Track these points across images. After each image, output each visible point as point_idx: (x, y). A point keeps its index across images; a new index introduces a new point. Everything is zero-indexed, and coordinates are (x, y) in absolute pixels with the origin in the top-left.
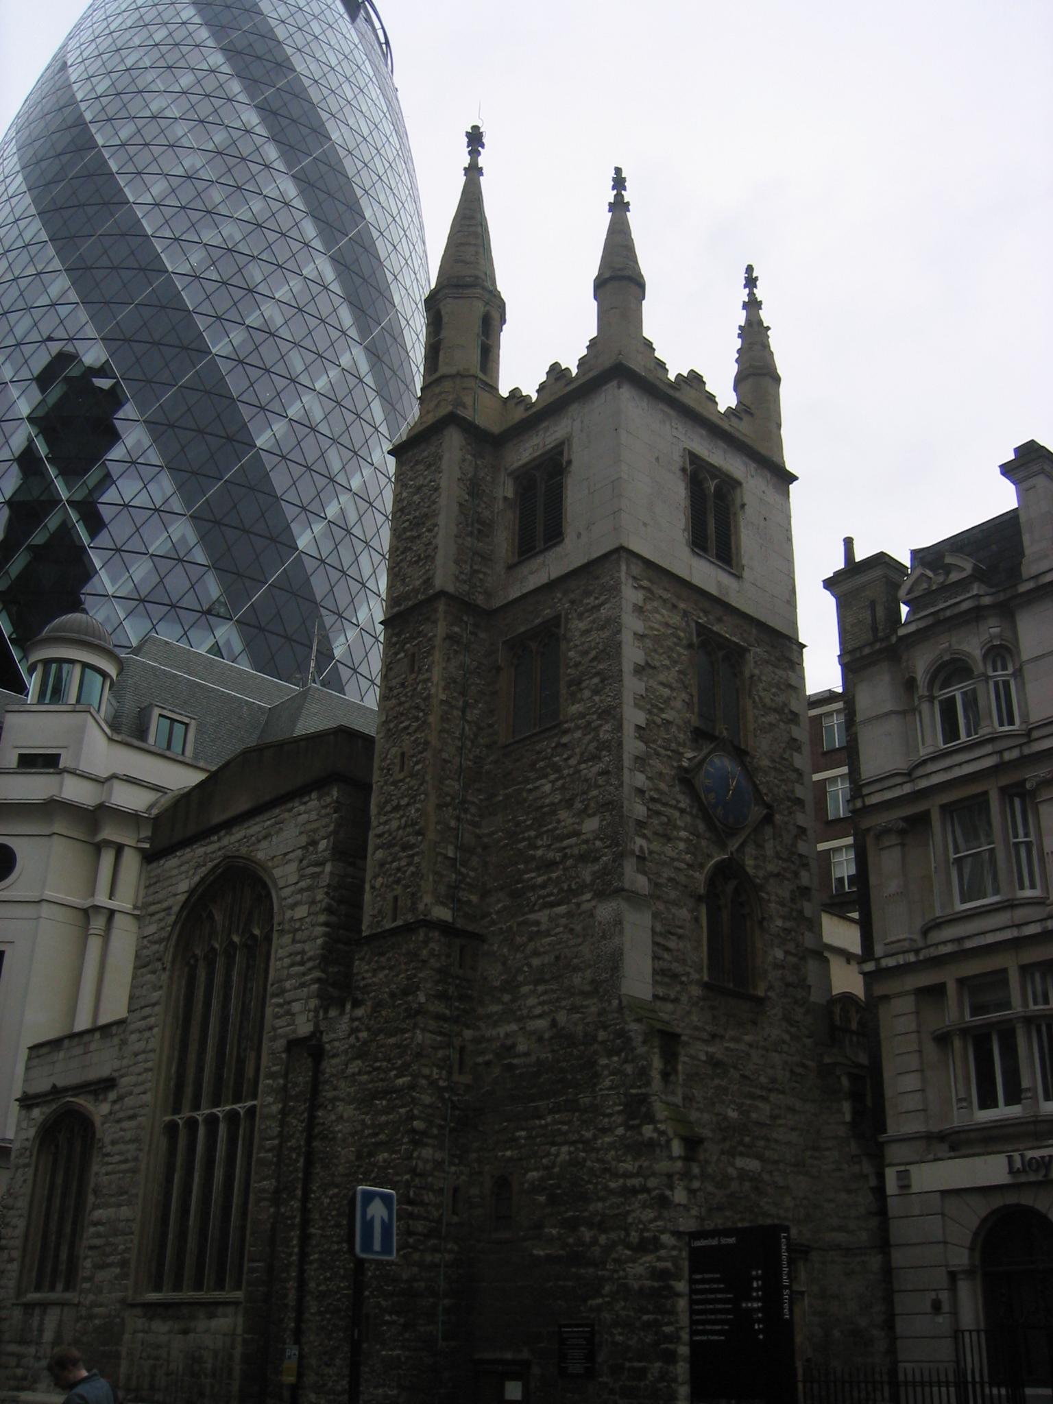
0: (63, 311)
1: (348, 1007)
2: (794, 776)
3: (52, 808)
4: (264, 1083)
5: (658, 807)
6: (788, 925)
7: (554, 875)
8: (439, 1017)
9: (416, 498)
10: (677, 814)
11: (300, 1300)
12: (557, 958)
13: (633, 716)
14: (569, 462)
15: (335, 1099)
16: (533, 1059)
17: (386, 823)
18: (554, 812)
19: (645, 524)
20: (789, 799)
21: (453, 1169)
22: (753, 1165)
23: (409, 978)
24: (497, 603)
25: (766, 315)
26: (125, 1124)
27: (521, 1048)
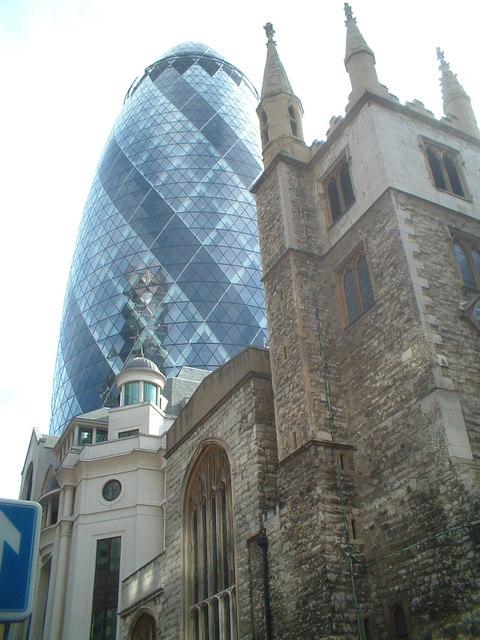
0: (131, 241)
1: (277, 508)
5: (446, 335)
7: (390, 395)
8: (334, 502)
9: (269, 208)
10: (463, 339)
12: (402, 446)
13: (419, 283)
14: (351, 158)
15: (279, 570)
16: (400, 517)
17: (282, 391)
18: (382, 357)
19: (403, 176)
21: (361, 605)
23: (309, 481)
24: (324, 252)
25: (453, 69)
26: (170, 616)
27: (391, 512)
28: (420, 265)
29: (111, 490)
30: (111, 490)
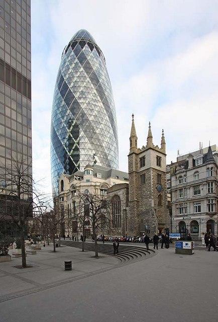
13: (152, 183)
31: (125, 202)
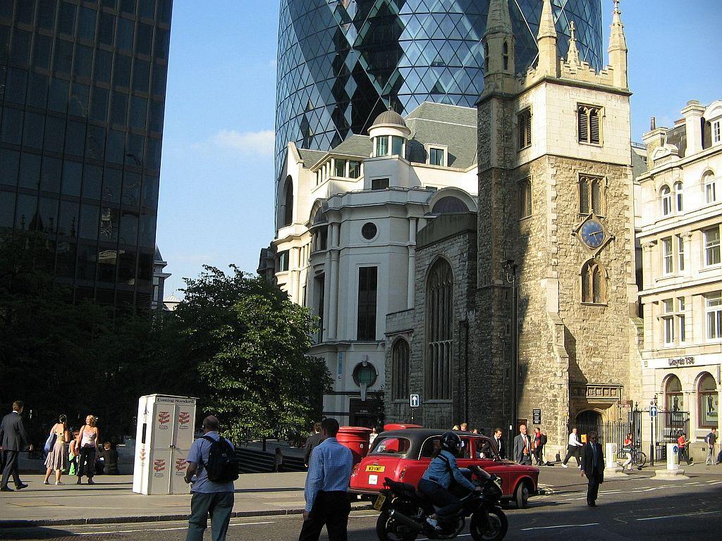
2: (624, 220)
3: (386, 206)
4: (454, 335)
6: (619, 277)
11: (467, 402)
20: (623, 230)
22: (599, 360)
28: (554, 205)
29: (369, 231)
30: (369, 231)
31: (464, 288)
